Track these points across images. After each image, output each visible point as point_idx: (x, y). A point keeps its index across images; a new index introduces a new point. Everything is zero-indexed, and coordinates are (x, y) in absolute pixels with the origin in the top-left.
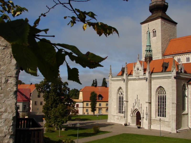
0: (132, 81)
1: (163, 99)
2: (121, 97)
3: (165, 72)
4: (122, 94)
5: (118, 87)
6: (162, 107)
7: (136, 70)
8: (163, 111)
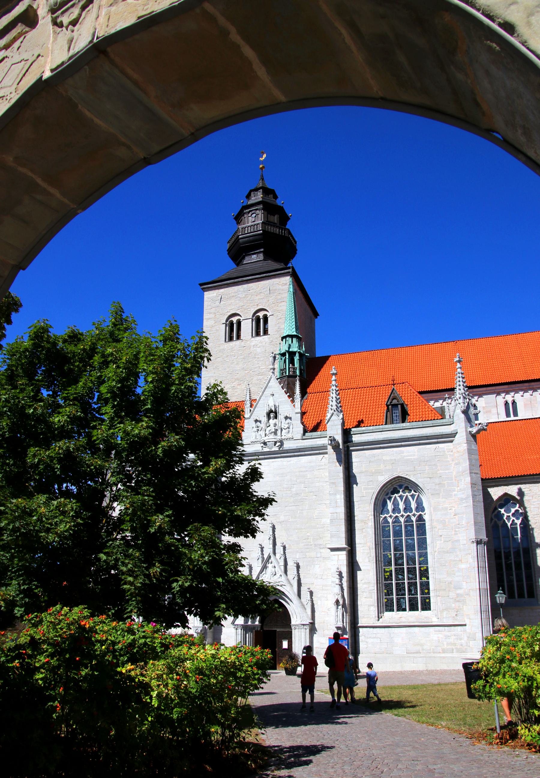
1: (409, 533)
6: (405, 567)
8: (413, 585)
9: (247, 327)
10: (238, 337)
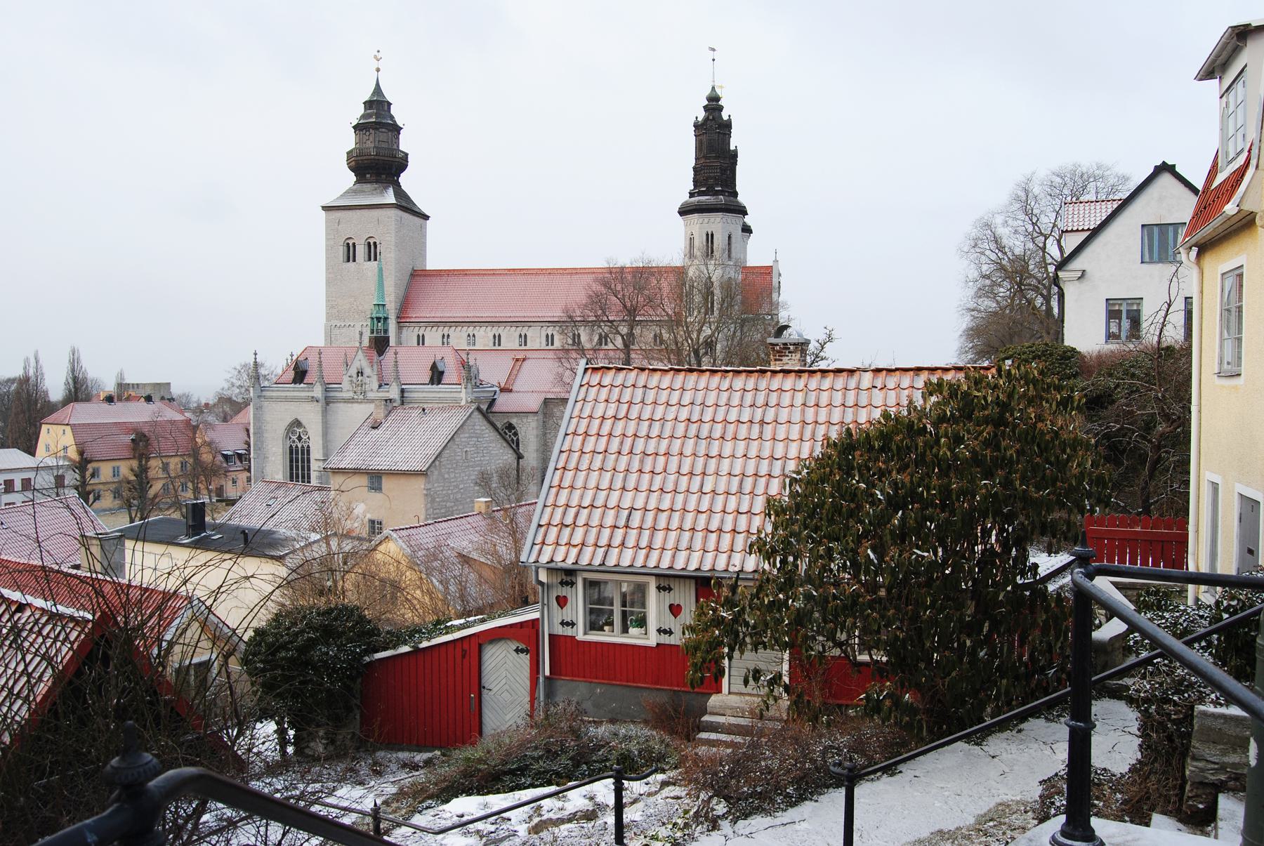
0: (341, 405)
2: (297, 447)
3: (439, 382)
4: (300, 438)
5: (289, 420)
7: (355, 376)
9: (361, 251)
10: (354, 261)
